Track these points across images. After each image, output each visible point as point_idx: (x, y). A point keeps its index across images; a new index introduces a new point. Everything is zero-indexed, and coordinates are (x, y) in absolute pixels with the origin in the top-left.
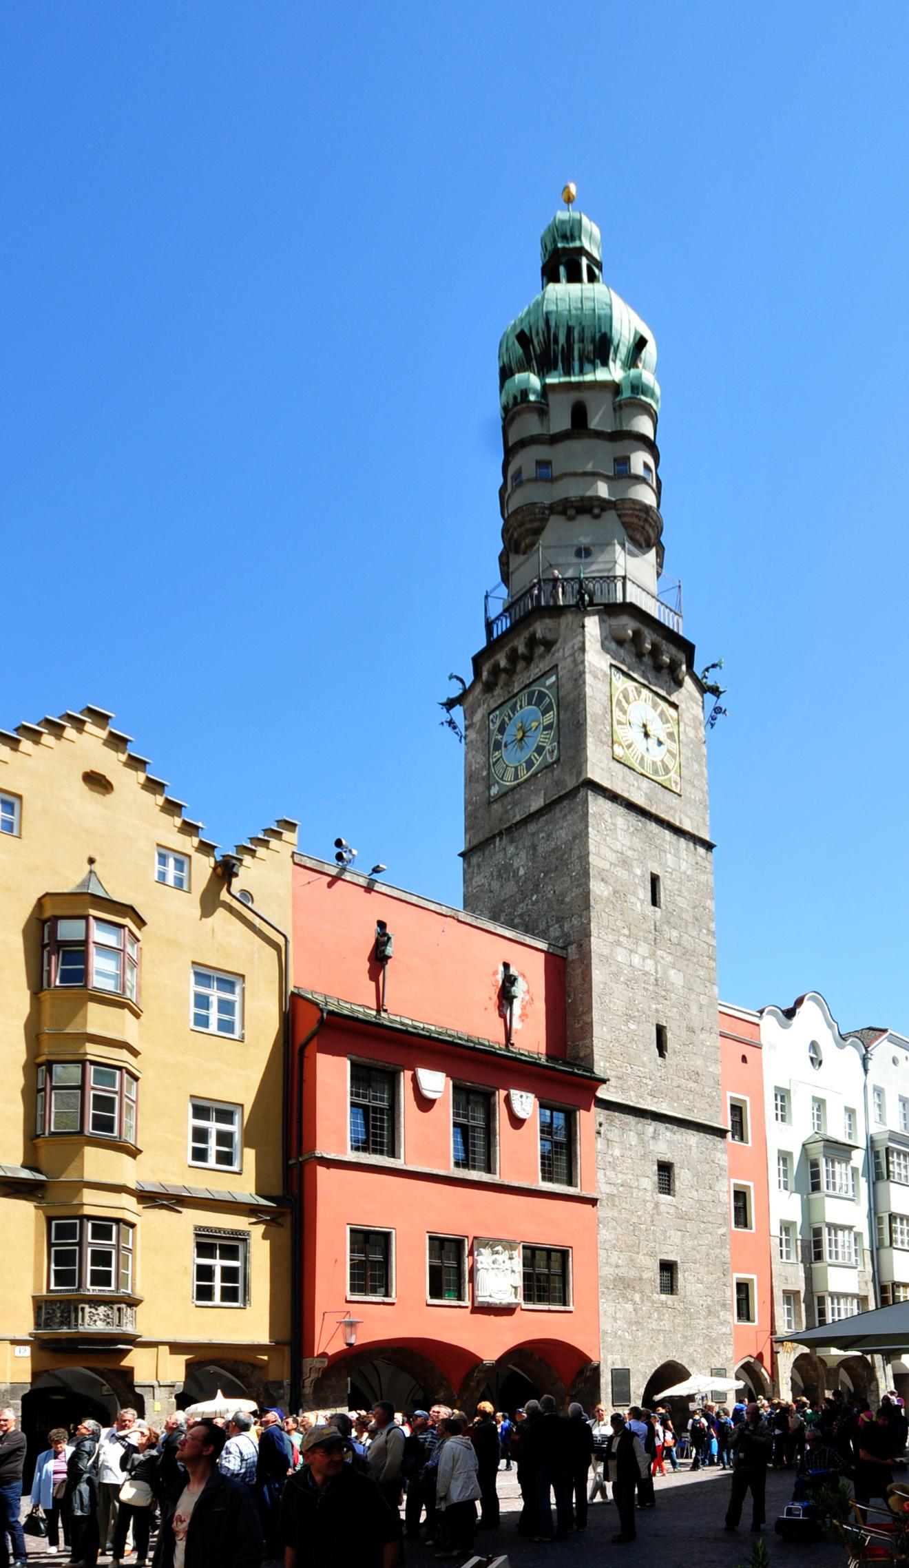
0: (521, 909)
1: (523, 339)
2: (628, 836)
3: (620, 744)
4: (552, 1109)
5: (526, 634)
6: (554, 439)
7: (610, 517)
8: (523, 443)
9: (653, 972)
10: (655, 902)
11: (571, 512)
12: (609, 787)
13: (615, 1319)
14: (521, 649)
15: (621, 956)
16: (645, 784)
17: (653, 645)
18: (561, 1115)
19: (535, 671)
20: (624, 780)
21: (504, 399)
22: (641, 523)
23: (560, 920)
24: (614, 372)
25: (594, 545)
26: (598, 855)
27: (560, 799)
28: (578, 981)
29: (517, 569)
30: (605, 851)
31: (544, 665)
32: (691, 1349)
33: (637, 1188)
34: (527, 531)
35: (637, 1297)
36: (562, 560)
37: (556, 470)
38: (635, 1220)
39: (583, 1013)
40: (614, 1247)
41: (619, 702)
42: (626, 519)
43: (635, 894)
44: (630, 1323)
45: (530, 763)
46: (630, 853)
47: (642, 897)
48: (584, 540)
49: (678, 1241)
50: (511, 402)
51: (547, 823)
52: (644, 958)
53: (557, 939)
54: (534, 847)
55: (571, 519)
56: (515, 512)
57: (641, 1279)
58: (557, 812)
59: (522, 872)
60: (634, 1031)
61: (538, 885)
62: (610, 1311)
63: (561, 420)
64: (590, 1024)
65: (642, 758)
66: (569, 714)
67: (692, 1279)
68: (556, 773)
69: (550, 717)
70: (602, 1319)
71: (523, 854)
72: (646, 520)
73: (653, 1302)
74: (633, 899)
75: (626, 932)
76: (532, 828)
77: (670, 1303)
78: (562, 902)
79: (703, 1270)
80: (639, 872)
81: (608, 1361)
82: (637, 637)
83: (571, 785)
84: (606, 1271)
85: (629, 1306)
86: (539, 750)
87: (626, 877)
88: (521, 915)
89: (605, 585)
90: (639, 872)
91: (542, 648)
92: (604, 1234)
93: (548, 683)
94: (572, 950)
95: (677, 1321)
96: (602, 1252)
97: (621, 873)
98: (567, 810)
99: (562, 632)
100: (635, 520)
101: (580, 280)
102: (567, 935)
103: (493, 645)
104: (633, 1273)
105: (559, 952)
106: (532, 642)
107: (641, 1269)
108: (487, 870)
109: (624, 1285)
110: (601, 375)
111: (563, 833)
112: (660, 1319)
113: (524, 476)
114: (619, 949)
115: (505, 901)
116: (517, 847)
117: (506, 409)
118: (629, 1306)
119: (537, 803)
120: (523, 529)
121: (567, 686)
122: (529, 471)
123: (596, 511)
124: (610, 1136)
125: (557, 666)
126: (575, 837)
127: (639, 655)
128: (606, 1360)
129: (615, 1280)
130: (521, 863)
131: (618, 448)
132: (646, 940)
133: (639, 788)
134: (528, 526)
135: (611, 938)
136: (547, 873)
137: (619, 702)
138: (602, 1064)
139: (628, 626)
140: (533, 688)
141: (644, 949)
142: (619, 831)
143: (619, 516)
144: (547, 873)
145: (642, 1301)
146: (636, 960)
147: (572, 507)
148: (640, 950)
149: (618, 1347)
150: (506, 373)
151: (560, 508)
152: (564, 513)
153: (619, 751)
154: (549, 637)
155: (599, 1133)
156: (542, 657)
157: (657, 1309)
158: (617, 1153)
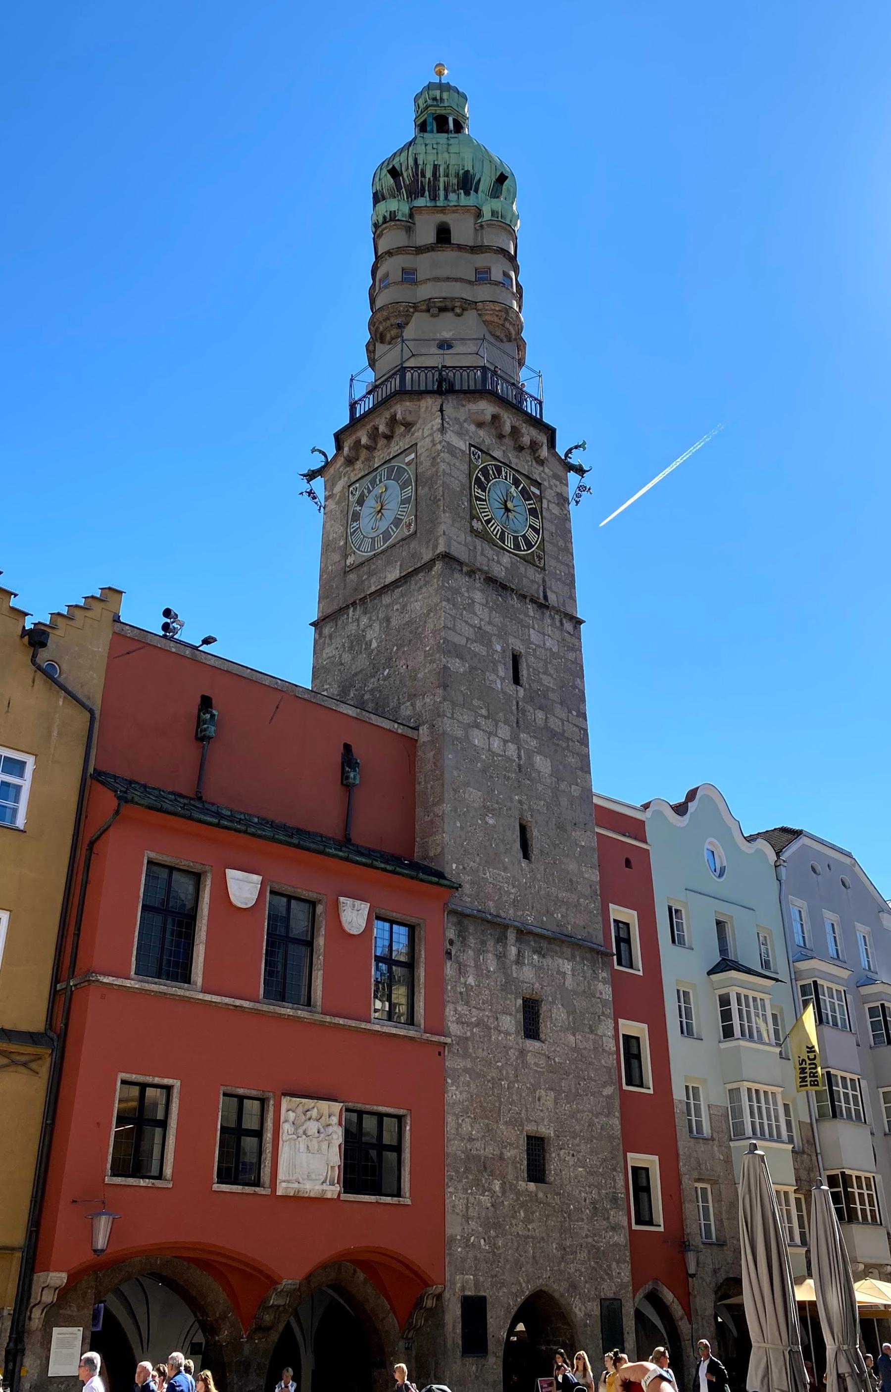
0: (372, 683)
1: (394, 173)
2: (486, 610)
3: (479, 519)
4: (392, 922)
5: (387, 414)
6: (420, 250)
7: (471, 315)
8: (389, 253)
9: (515, 757)
10: (516, 680)
11: (436, 311)
12: (467, 561)
13: (467, 1219)
14: (382, 428)
15: (478, 739)
16: (506, 559)
17: (513, 427)
18: (403, 930)
19: (395, 449)
20: (482, 554)
21: (375, 218)
22: (501, 322)
23: (412, 697)
24: (480, 198)
25: (455, 340)
26: (454, 629)
27: (416, 571)
28: (429, 767)
29: (380, 357)
30: (460, 625)
31: (404, 443)
32: (572, 1268)
33: (496, 1028)
34: (392, 325)
35: (497, 1185)
36: (424, 351)
37: (421, 276)
38: (494, 1073)
39: (435, 804)
40: (465, 1111)
41: (477, 478)
42: (487, 318)
43: (495, 671)
44: (488, 1224)
45: (386, 535)
46: (488, 628)
47: (502, 673)
48: (447, 335)
49: (550, 1104)
50: (381, 220)
51: (402, 595)
52: (505, 742)
53: (409, 718)
54: (388, 620)
55: (433, 316)
56: (381, 308)
57: (501, 1158)
58: (413, 585)
59: (374, 644)
60: (494, 826)
61: (391, 659)
62: (460, 1206)
63: (426, 234)
64: (442, 817)
65: (503, 532)
66: (426, 489)
67: (571, 1161)
68: (412, 546)
69: (409, 491)
70: (448, 1217)
71: (376, 626)
72: (506, 319)
73: (518, 1194)
74: (493, 677)
75: (484, 712)
76: (386, 599)
77: (541, 1195)
78: (415, 678)
79: (584, 1148)
80: (498, 648)
81: (458, 1283)
82: (495, 417)
83: (427, 556)
84: (454, 1147)
85: (485, 1200)
86: (397, 522)
87: (484, 653)
88: (372, 691)
89: (465, 373)
90: (498, 648)
91: (403, 428)
92: (454, 1094)
93: (407, 460)
94: (424, 730)
95: (551, 1223)
96: (450, 1119)
97: (476, 647)
98: (422, 582)
99: (422, 415)
100: (496, 319)
101: (447, 131)
102: (420, 715)
103: (355, 422)
104: (491, 1150)
105: (410, 733)
106: (393, 421)
107: (503, 1145)
108: (338, 641)
109: (482, 1168)
110: (464, 200)
111: (417, 605)
112: (528, 1220)
113: (391, 279)
114: (476, 732)
115: (356, 674)
116: (370, 619)
117: (376, 226)
118: (485, 1200)
119: (393, 575)
120: (388, 322)
121: (426, 463)
122: (397, 276)
123: (458, 311)
124: (463, 958)
125: (416, 444)
126: (430, 611)
127: (501, 437)
128: (454, 1284)
129: (468, 1158)
130: (374, 635)
131: (481, 260)
132: (506, 722)
133: (498, 562)
134: (394, 321)
135: (467, 718)
136: (400, 647)
137: (477, 478)
138: (454, 866)
139: (486, 408)
140: (393, 463)
141: (504, 731)
142: (477, 606)
143: (480, 315)
144: (400, 647)
145: (504, 1192)
146: (496, 744)
147: (435, 307)
148: (500, 733)
149: (470, 1262)
150: (377, 198)
151: (424, 307)
152: (428, 311)
153: (476, 525)
154: (409, 419)
155: (449, 954)
156: (403, 435)
157: (523, 1205)
158: (471, 980)
